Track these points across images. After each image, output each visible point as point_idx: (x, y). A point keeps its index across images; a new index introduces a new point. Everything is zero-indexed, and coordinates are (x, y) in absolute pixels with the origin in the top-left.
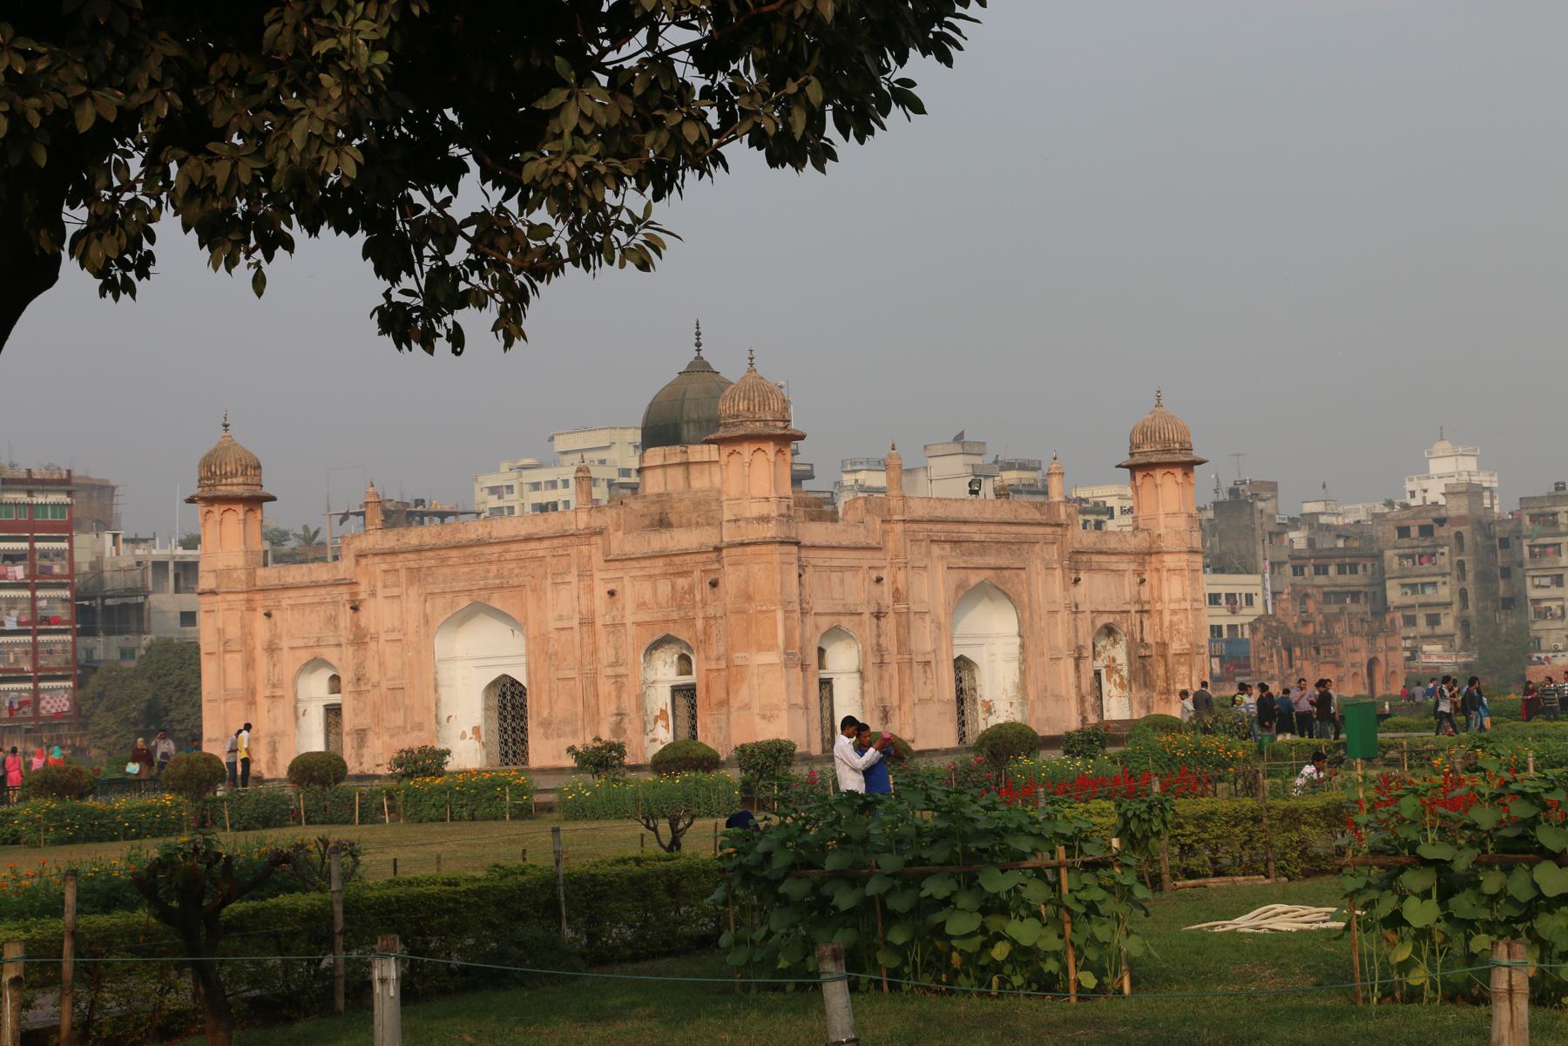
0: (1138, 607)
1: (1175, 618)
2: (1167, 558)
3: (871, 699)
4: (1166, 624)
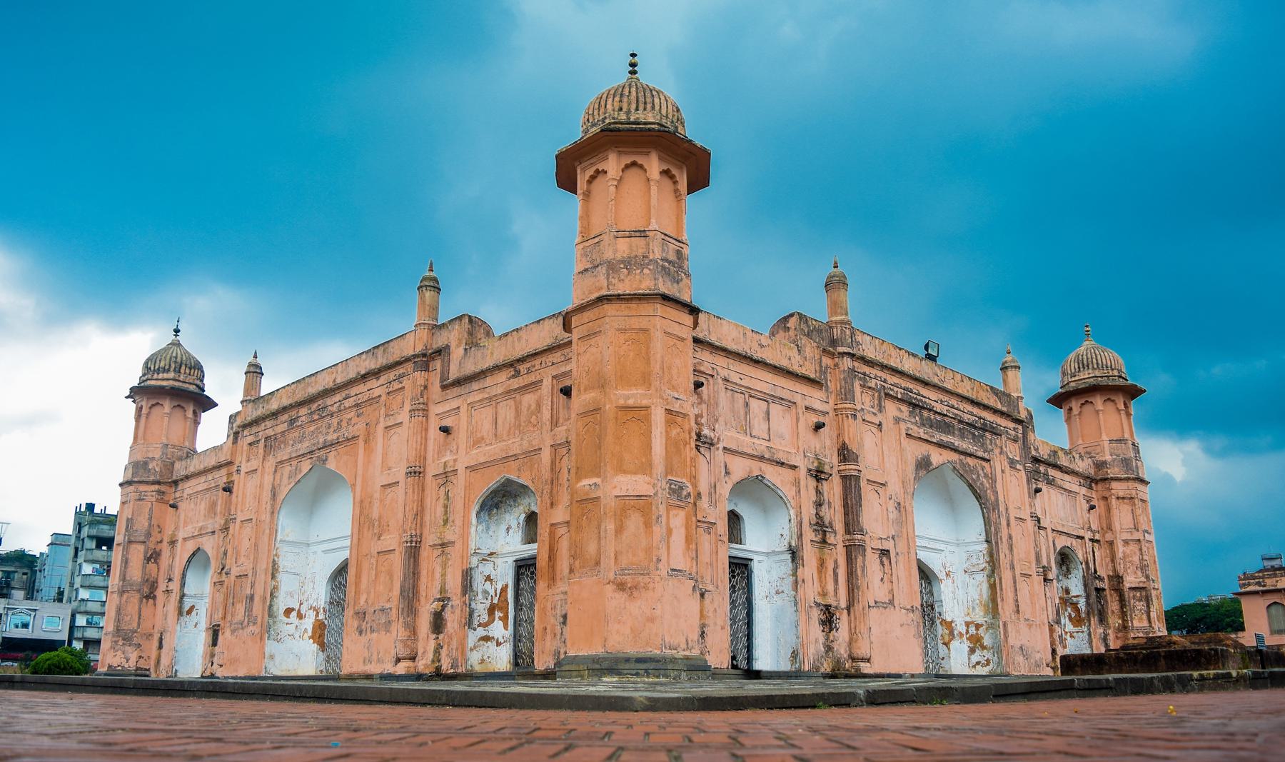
0: (1088, 535)
1: (1129, 550)
2: (1114, 485)
3: (811, 592)
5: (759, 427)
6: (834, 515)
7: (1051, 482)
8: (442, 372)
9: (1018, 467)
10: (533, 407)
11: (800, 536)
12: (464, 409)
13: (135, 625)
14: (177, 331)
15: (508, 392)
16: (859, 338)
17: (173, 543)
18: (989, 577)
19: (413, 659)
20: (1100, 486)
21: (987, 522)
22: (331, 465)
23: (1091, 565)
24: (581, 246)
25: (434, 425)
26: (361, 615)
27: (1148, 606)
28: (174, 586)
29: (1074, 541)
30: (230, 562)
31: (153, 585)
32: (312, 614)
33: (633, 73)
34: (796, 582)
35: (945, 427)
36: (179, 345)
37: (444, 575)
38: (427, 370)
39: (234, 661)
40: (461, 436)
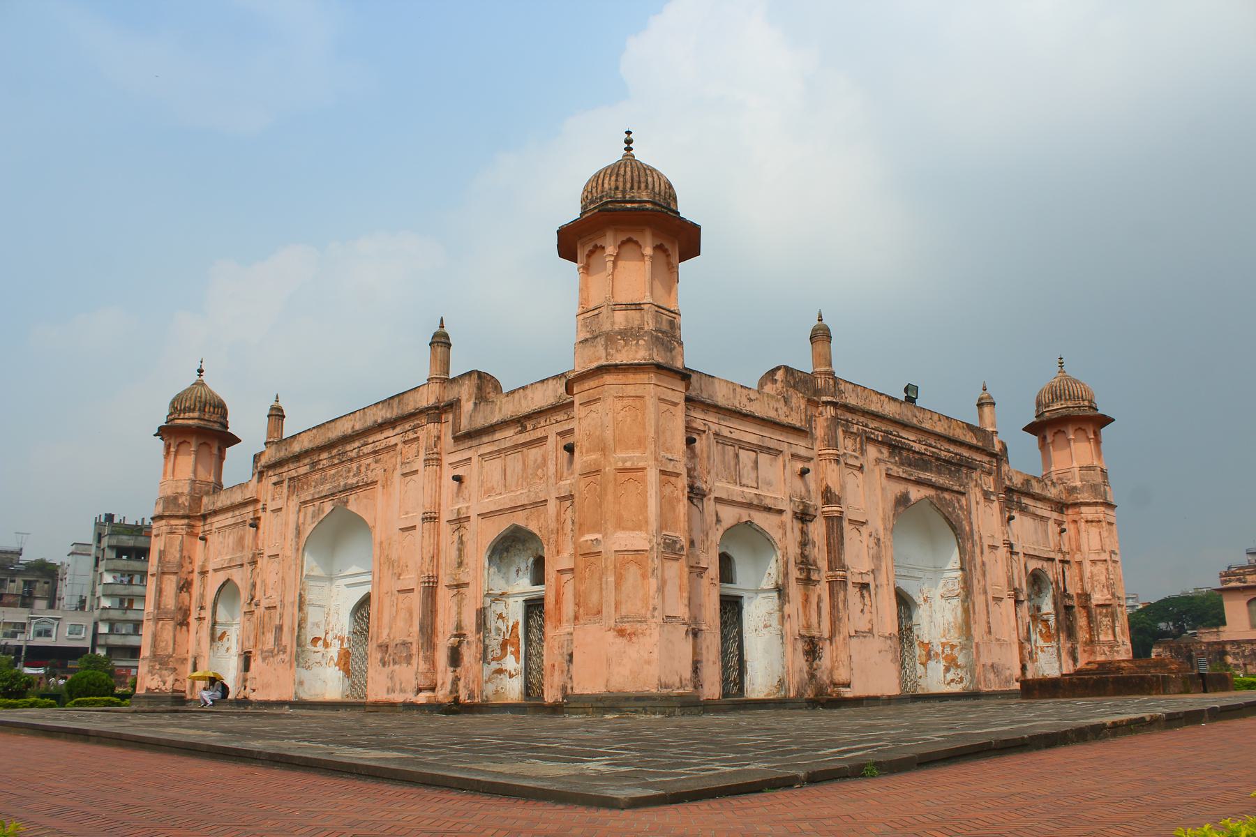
0: (1058, 557)
2: (1084, 509)
3: (795, 626)
4: (1087, 574)
5: (748, 476)
6: (819, 554)
7: (1023, 510)
8: (454, 424)
9: (993, 498)
10: (540, 460)
11: (786, 575)
12: (475, 460)
13: (170, 650)
14: (200, 371)
15: (516, 446)
16: (842, 387)
17: (203, 573)
18: (963, 601)
19: (433, 689)
20: (1070, 511)
21: (962, 551)
22: (352, 507)
23: (1061, 585)
24: (581, 317)
25: (448, 473)
26: (384, 647)
27: (1113, 622)
28: (207, 614)
29: (1045, 564)
30: (259, 595)
31: (186, 612)
32: (337, 643)
33: (629, 149)
34: (783, 617)
35: (922, 462)
36: (202, 384)
37: (459, 613)
38: (439, 421)
39: (266, 686)
40: (472, 483)
